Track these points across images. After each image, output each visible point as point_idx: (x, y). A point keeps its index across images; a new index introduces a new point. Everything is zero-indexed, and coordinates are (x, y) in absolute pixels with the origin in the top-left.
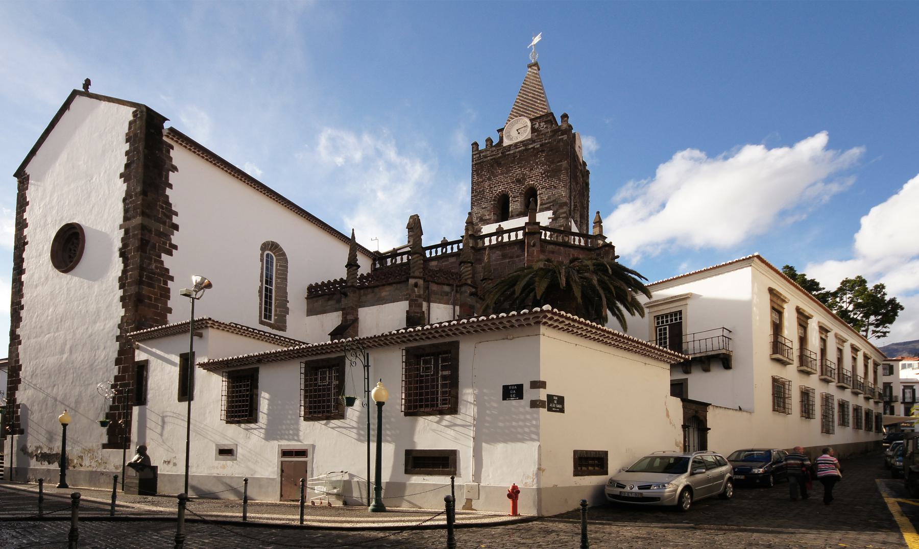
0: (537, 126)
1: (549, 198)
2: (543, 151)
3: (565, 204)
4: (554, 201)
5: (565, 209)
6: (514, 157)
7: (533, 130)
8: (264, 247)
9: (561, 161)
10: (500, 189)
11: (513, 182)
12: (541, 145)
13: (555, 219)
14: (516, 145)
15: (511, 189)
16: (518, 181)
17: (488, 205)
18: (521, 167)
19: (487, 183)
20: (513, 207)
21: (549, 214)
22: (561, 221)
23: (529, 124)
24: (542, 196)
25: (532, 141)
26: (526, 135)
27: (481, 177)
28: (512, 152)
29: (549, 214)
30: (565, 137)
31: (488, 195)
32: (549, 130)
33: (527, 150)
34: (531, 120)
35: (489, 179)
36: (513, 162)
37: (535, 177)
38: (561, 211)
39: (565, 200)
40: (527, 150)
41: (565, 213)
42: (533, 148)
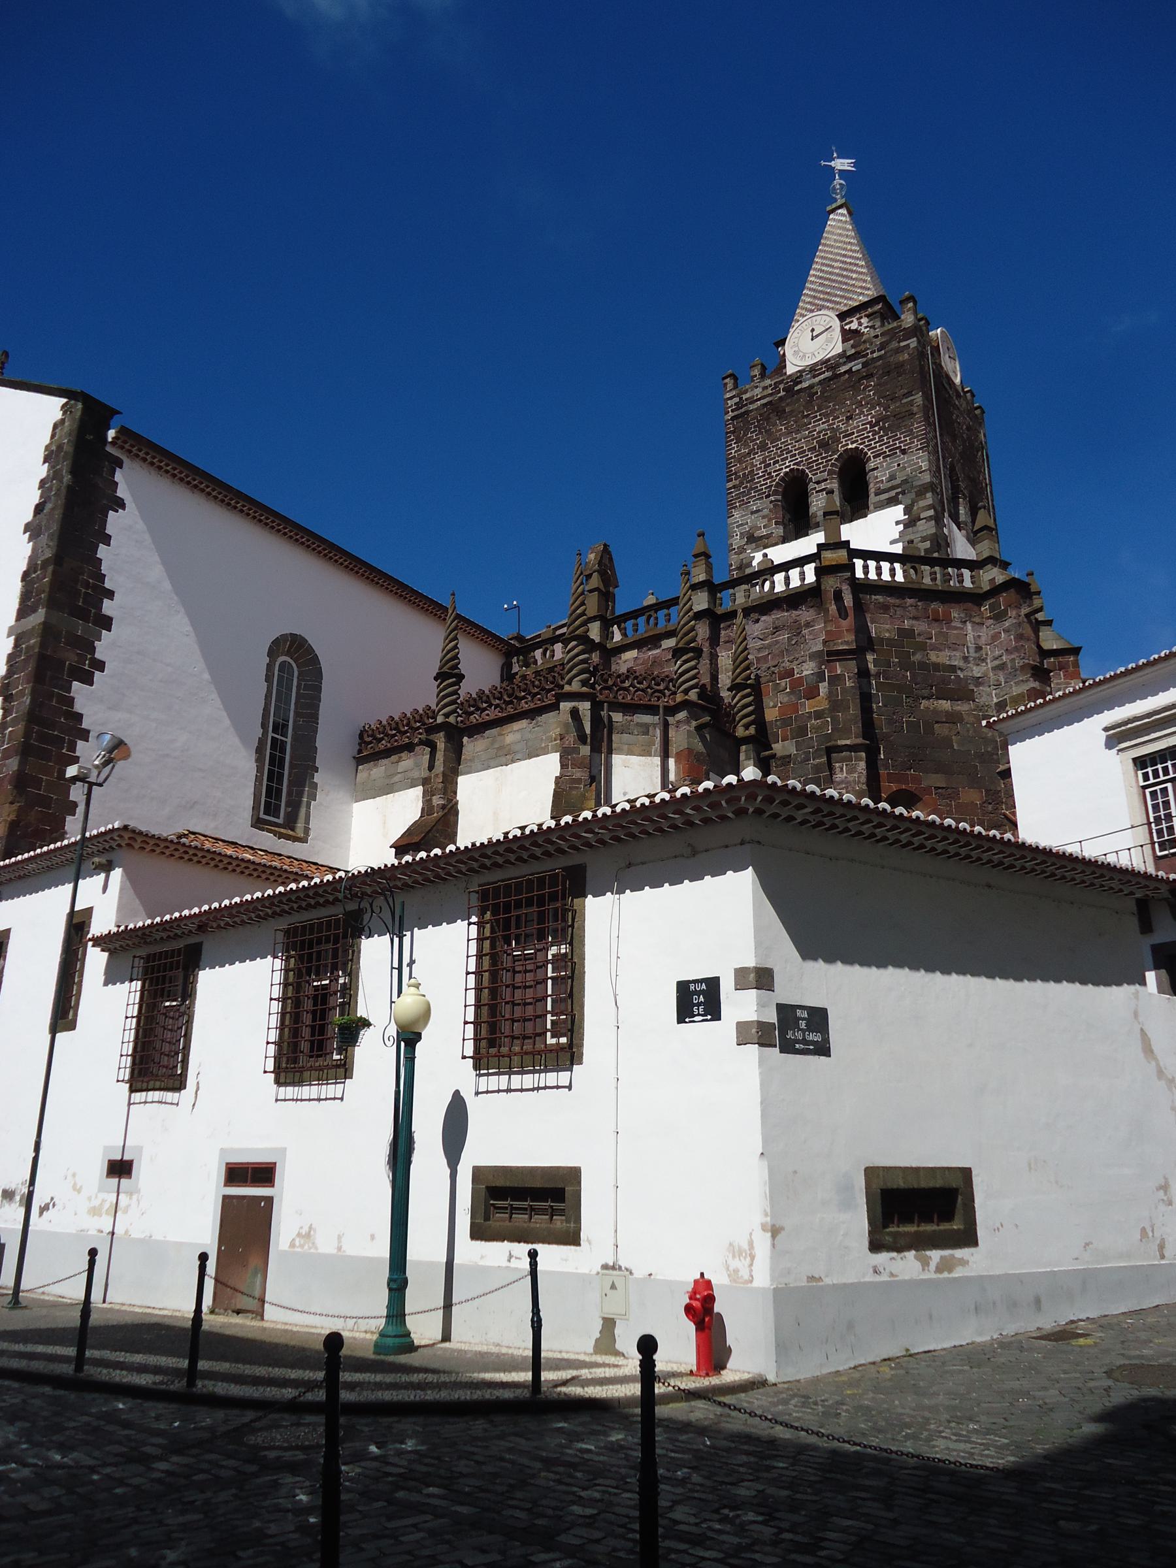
0: (854, 326)
1: (892, 477)
2: (869, 376)
3: (931, 487)
4: (905, 482)
5: (929, 499)
6: (812, 395)
7: (847, 335)
8: (275, 648)
9: (909, 394)
10: (786, 466)
11: (812, 449)
12: (865, 365)
13: (910, 523)
14: (813, 370)
15: (809, 463)
16: (824, 445)
17: (765, 505)
18: (826, 415)
19: (758, 458)
20: (817, 504)
21: (898, 512)
22: (926, 528)
23: (836, 323)
24: (880, 472)
25: (844, 357)
26: (832, 345)
27: (746, 445)
28: (805, 385)
29: (898, 512)
30: (913, 342)
31: (762, 483)
32: (878, 332)
33: (836, 377)
34: (842, 316)
35: (763, 447)
36: (809, 404)
37: (857, 430)
38: (922, 503)
39: (927, 478)
40: (836, 377)
41: (929, 507)
42: (850, 371)
